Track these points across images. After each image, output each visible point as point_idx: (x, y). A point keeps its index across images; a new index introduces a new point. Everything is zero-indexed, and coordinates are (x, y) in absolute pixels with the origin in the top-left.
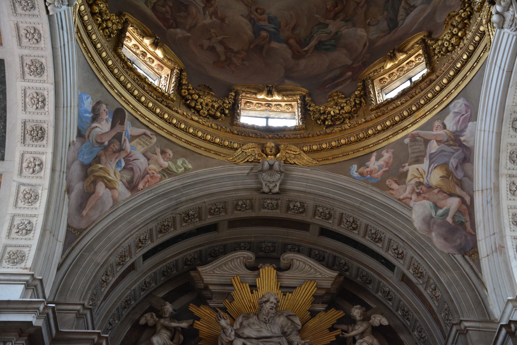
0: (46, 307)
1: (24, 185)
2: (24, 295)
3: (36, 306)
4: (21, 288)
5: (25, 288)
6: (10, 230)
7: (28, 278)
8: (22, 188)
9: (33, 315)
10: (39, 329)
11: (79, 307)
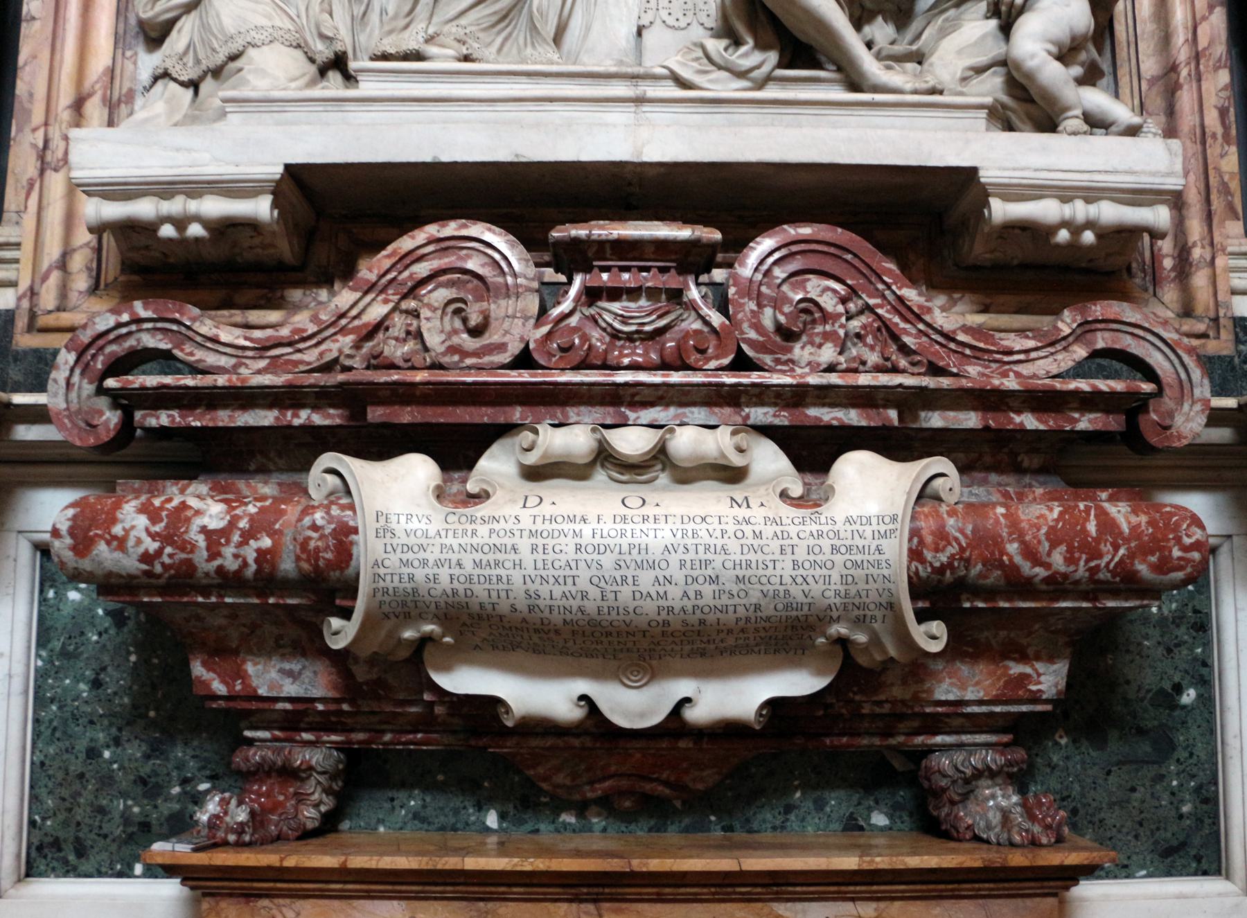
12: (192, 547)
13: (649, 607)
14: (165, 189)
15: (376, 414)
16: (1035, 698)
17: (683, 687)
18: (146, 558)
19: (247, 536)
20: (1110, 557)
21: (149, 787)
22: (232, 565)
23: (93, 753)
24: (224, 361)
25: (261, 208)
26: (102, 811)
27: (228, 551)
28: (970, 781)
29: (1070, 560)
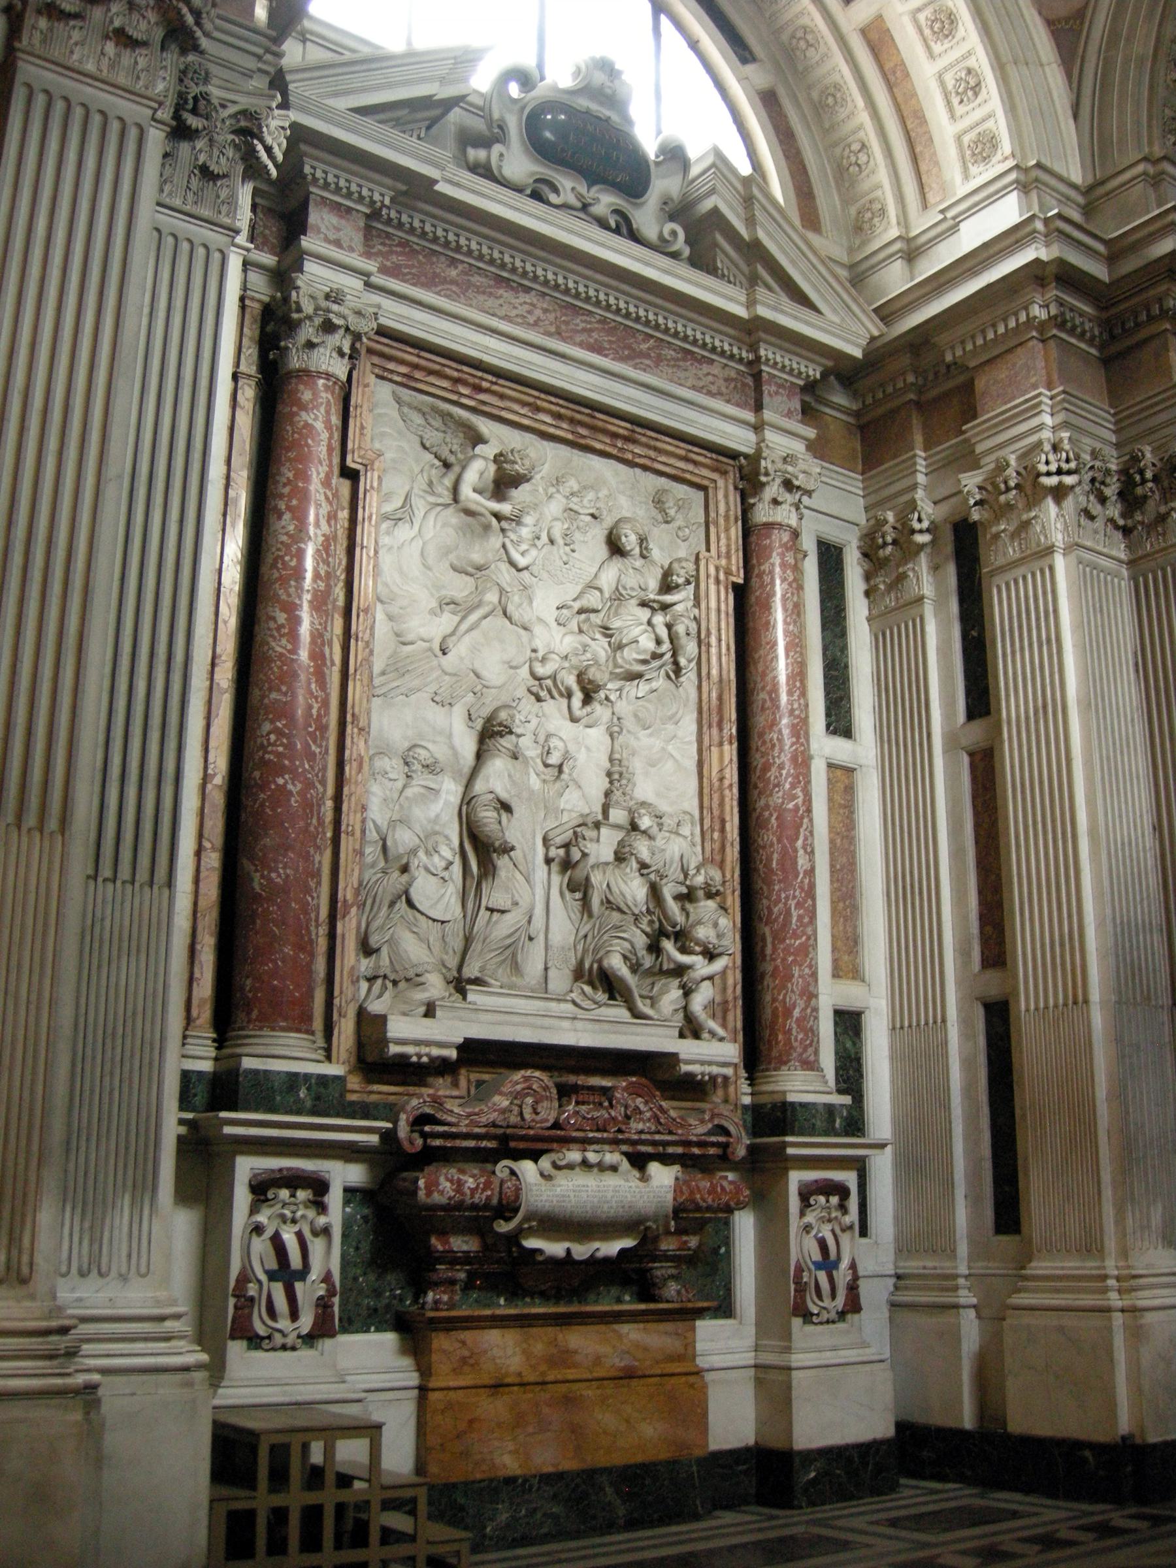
0: (1047, 221)
1: (919, 10)
2: (1024, 205)
3: (1028, 229)
4: (1013, 200)
5: (1022, 194)
6: (949, 103)
7: (1013, 176)
8: (922, 17)
9: (1034, 246)
10: (1061, 262)
11: (1140, 168)
12: (463, 1194)
13: (604, 1216)
14: (417, 1043)
15: (512, 1144)
16: (689, 1249)
17: (597, 1245)
18: (450, 1198)
19: (484, 1190)
20: (725, 1199)
21: (377, 1293)
22: (476, 1200)
23: (355, 1279)
24: (454, 1120)
25: (453, 1054)
26: (358, 1305)
27: (477, 1196)
28: (665, 1280)
29: (713, 1201)
